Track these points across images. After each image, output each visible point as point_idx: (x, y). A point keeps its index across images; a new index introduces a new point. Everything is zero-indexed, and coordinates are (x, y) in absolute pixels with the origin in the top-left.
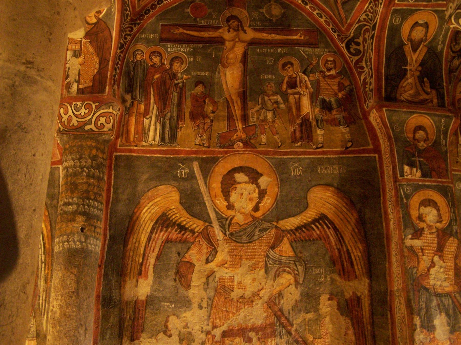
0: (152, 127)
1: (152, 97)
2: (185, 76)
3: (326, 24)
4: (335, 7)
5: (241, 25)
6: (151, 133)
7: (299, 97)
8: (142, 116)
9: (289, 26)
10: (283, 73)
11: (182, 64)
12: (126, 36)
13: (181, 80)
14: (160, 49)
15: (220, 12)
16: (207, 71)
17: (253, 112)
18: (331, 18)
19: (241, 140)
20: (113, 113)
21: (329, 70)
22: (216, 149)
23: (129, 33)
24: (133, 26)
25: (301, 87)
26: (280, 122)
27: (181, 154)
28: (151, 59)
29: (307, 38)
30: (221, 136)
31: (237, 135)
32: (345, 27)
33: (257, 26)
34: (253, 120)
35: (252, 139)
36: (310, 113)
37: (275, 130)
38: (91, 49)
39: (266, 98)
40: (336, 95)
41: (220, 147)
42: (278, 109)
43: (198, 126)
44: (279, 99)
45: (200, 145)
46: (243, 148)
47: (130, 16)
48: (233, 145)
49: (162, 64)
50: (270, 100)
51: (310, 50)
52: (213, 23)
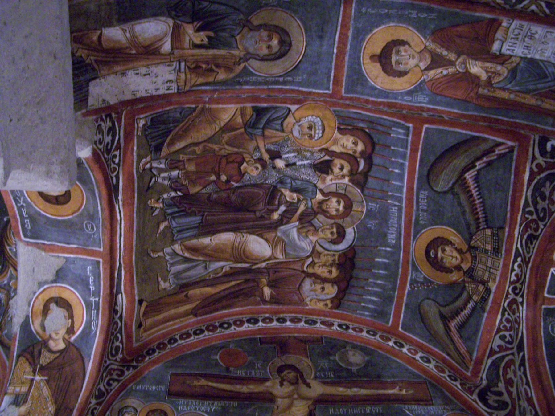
3: (439, 371)
4: (448, 342)
5: (302, 376)
9: (379, 376)
12: (111, 382)
18: (444, 361)
23: (116, 377)
24: (125, 369)
29: (411, 392)
32: (471, 368)
33: (328, 378)
38: (46, 392)
47: (122, 353)
52: (256, 374)
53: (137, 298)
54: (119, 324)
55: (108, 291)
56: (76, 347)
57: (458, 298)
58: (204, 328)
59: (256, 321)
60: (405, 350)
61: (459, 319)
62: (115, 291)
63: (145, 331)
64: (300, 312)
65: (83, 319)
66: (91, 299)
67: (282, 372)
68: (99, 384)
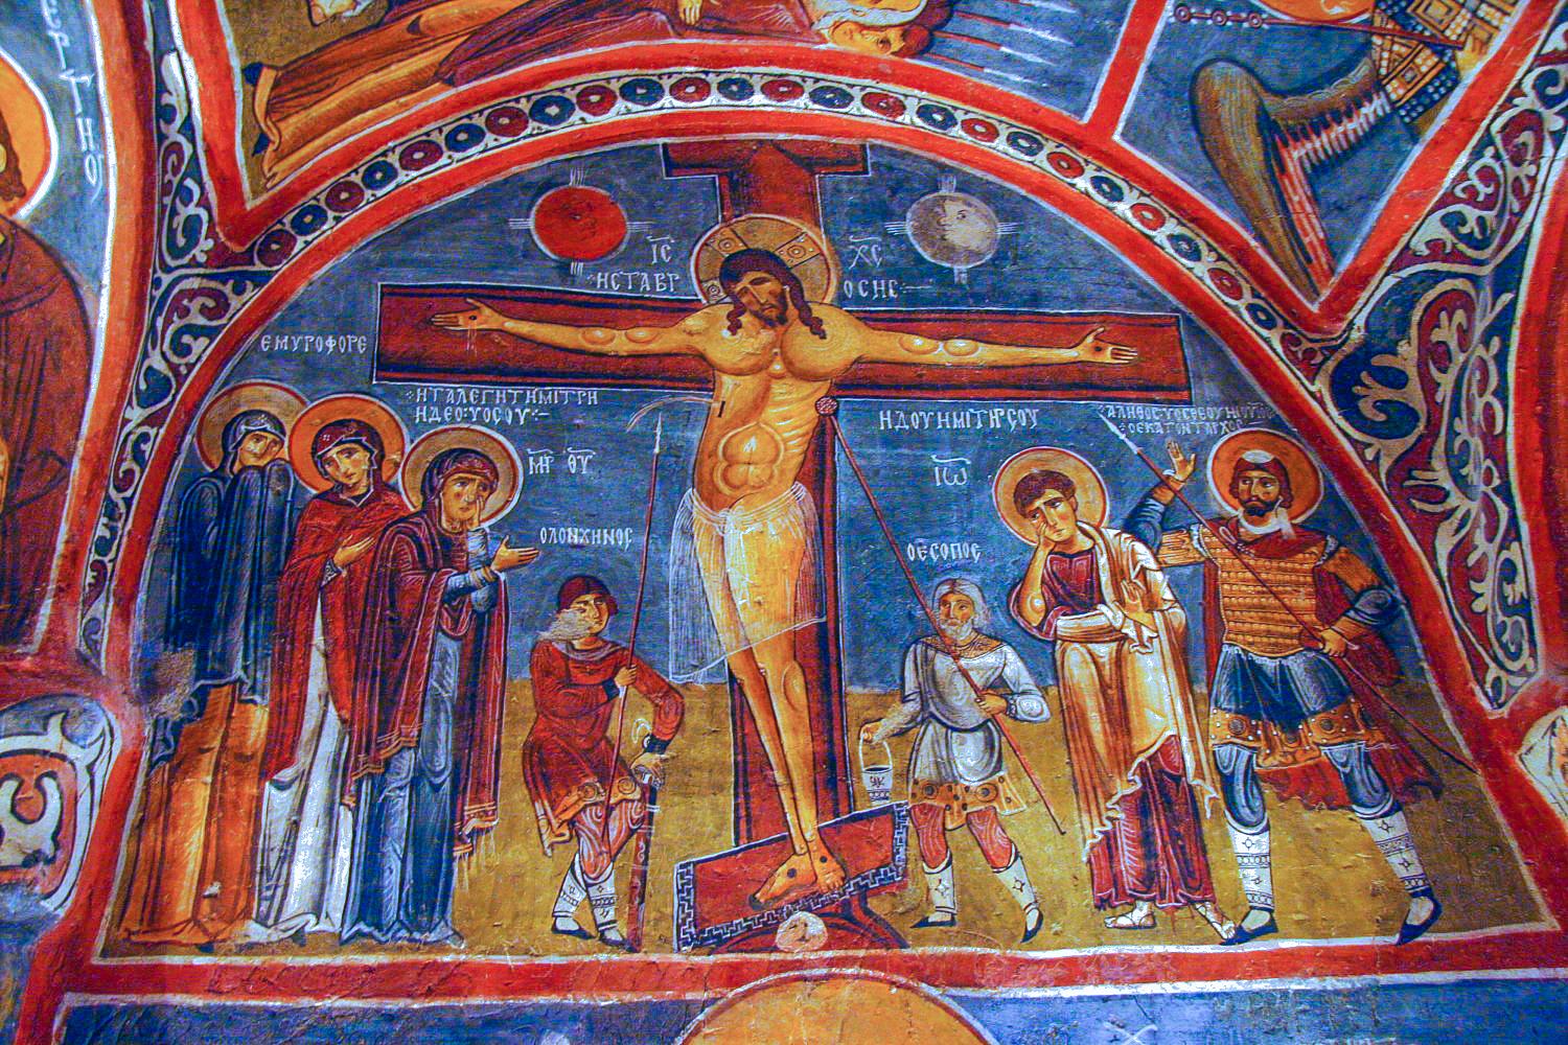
0: (310, 836)
1: (317, 663)
2: (504, 552)
3: (1221, 287)
4: (1267, 201)
6: (302, 873)
7: (1119, 651)
8: (253, 769)
10: (1027, 532)
11: (489, 487)
12: (186, 339)
13: (481, 573)
14: (377, 411)
15: (687, 234)
16: (623, 524)
17: (876, 739)
18: (1242, 254)
19: (811, 900)
20: (63, 758)
21: (1258, 512)
22: (676, 958)
23: (202, 321)
24: (228, 289)
25: (1121, 602)
26: (1025, 794)
27: (471, 992)
28: (321, 463)
29: (1130, 355)
30: (705, 882)
31: (792, 873)
32: (1325, 294)
33: (879, 302)
34: (877, 782)
35: (877, 893)
36: (1185, 740)
37: (999, 840)
39: (943, 664)
40: (1309, 639)
41: (699, 944)
42: (1008, 723)
43: (571, 823)
44: (1012, 664)
45: (581, 934)
46: (827, 947)
47: (211, 233)
48: (770, 929)
49: (382, 487)
50: (965, 674)
51: (1147, 416)
52: (656, 285)
53: (236, 63)
54: (188, 149)
55: (122, 51)
56: (40, 243)
57: (1330, 77)
58: (480, 121)
59: (653, 92)
60: (1123, 208)
61: (1321, 143)
62: (149, 46)
63: (281, 157)
64: (797, 63)
65: (47, 145)
66: (63, 77)
67: (737, 280)
68: (146, 355)
